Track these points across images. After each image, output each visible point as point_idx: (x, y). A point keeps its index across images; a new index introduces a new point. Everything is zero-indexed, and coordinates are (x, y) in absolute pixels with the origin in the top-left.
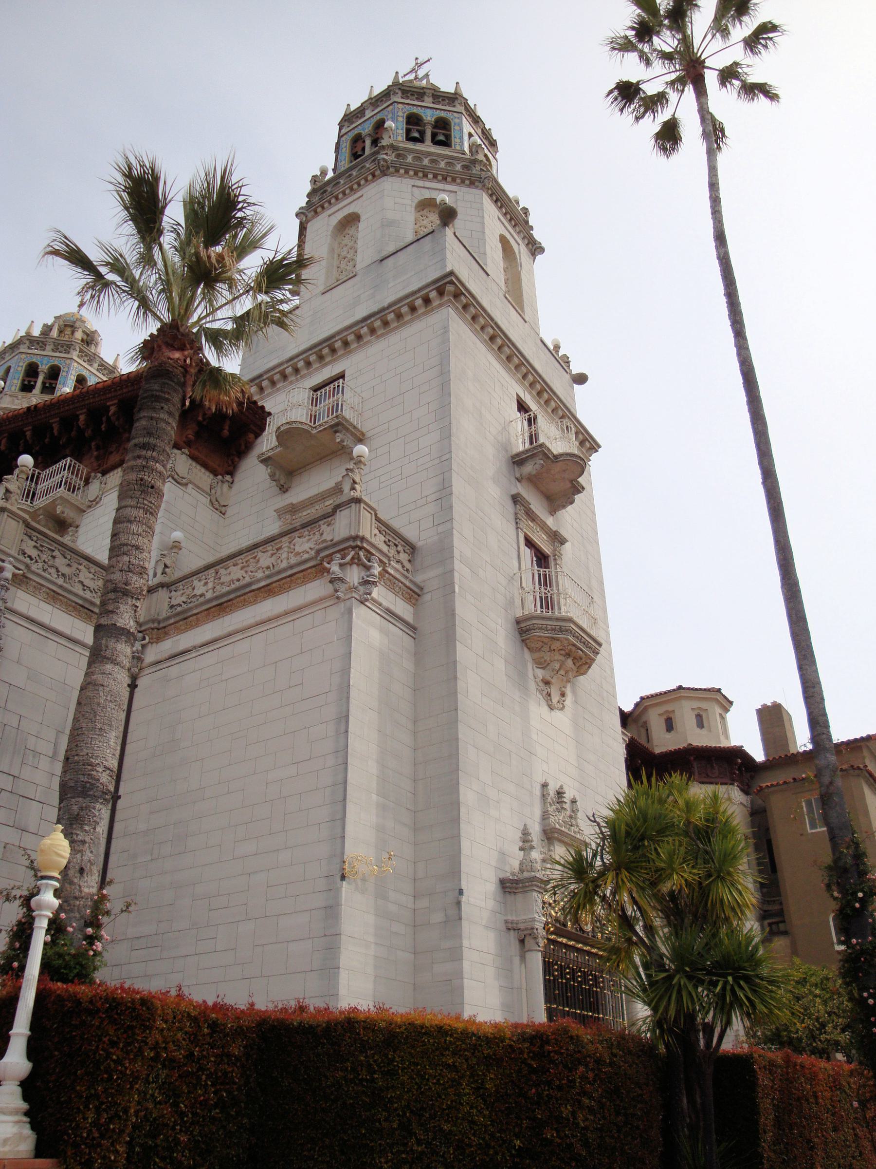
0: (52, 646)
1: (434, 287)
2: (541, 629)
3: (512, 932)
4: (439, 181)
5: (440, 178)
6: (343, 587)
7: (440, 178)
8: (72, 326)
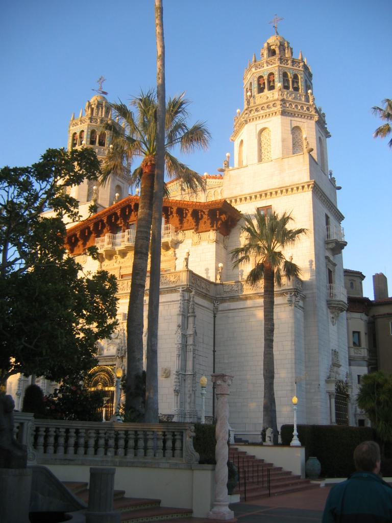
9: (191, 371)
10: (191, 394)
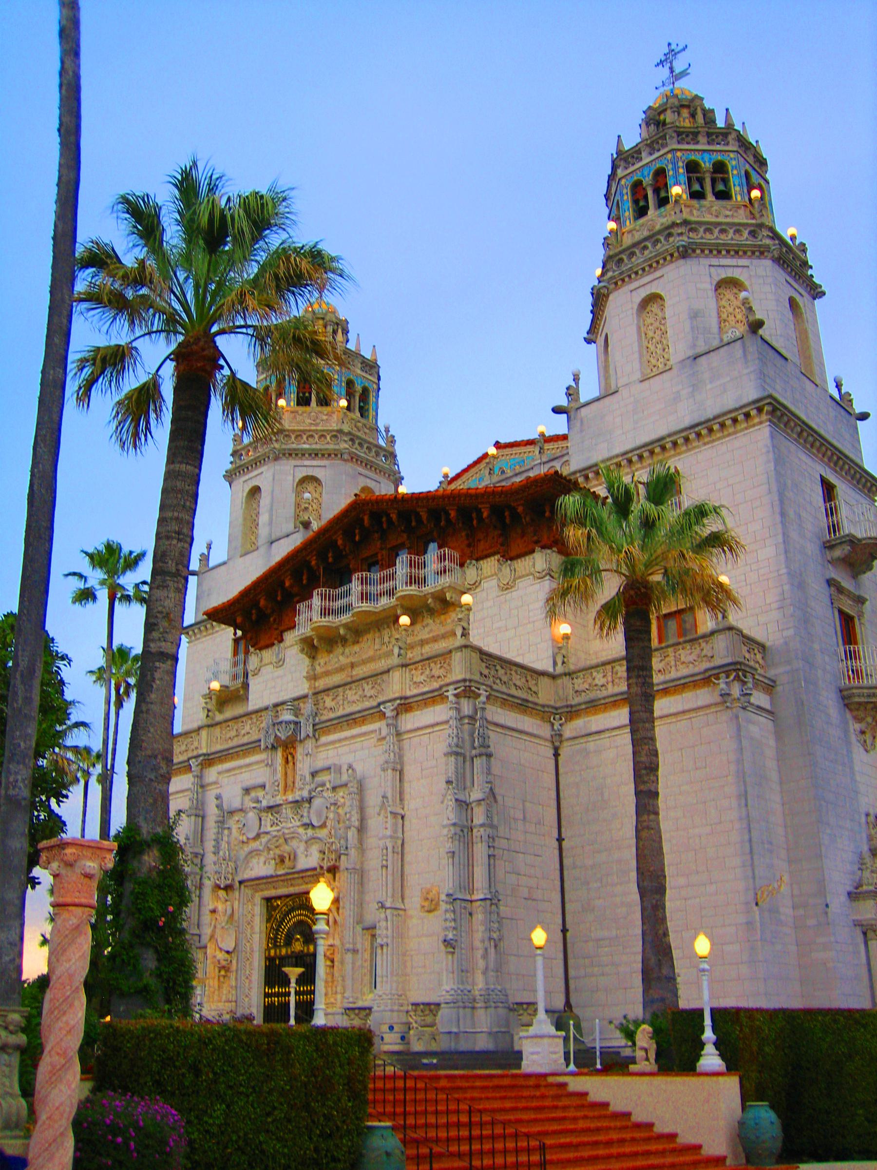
1: (753, 407)
2: (859, 696)
3: (857, 927)
4: (732, 257)
5: (732, 253)
6: (730, 699)
7: (732, 253)
8: (323, 319)
9: (486, 891)
10: (486, 949)
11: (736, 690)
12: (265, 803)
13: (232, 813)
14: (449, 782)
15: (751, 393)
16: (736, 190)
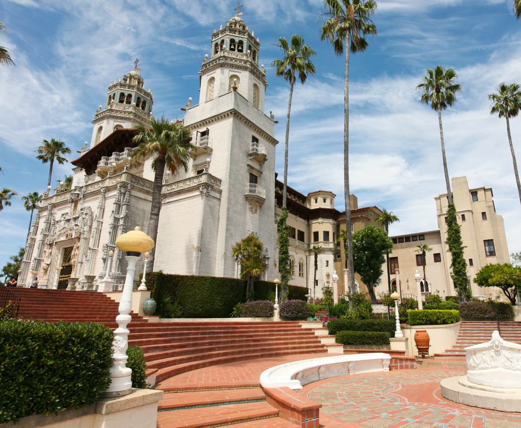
0: (140, 202)
11: (205, 191)
12: (67, 218)
13: (57, 222)
14: (113, 212)
15: (231, 107)
16: (245, 49)
